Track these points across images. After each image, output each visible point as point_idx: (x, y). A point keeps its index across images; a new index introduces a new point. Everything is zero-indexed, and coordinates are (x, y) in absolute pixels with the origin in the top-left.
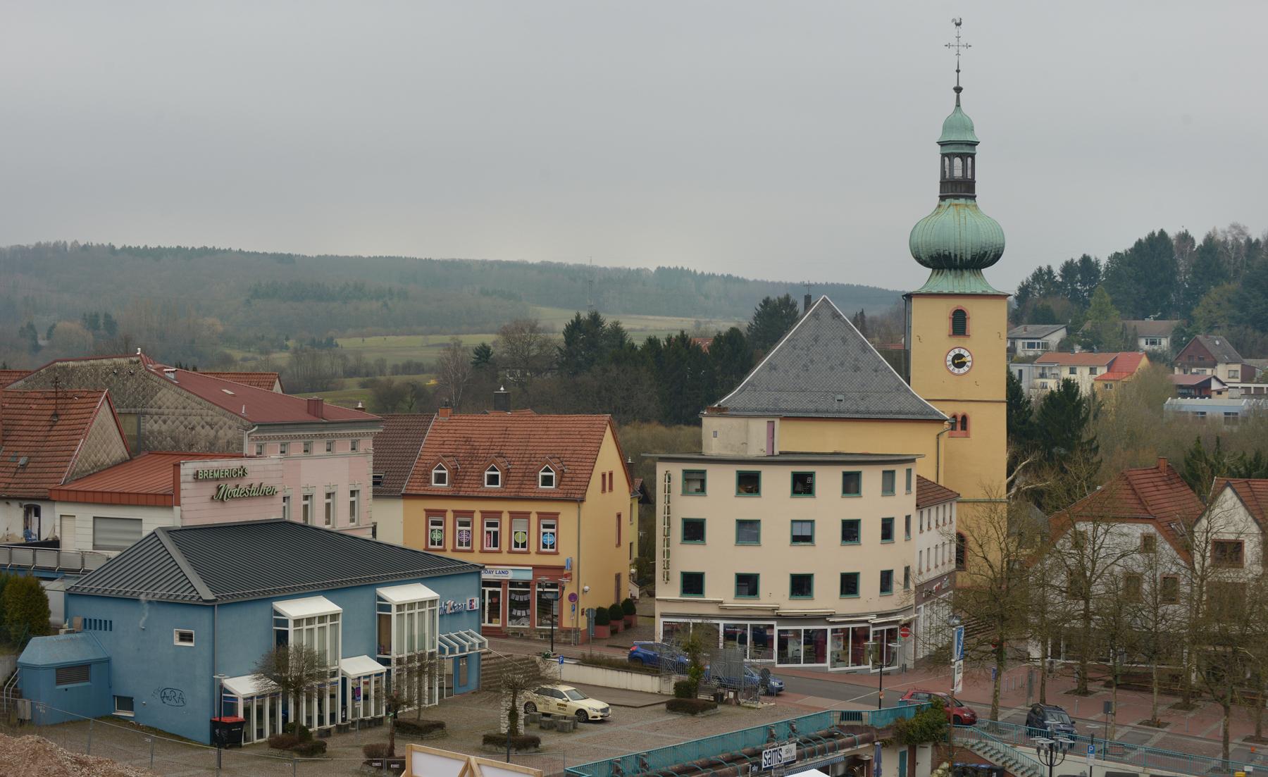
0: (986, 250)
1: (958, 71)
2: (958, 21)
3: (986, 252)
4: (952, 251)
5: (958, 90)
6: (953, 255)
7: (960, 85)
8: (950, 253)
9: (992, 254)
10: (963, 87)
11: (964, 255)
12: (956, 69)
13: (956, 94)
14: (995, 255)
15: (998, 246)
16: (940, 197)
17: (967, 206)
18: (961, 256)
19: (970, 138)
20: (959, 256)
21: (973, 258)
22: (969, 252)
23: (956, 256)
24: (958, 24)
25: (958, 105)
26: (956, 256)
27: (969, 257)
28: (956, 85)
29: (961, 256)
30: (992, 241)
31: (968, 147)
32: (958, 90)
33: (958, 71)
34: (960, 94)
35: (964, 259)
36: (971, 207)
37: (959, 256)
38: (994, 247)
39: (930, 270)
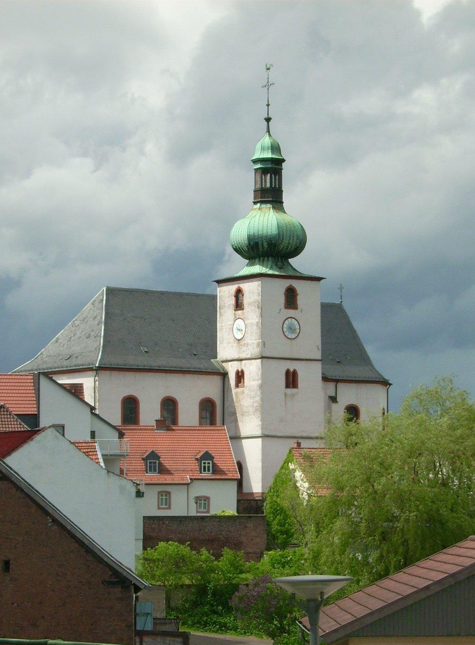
0: (257, 241)
2: (268, 66)
3: (257, 244)
5: (268, 120)
6: (238, 248)
9: (265, 244)
10: (272, 117)
14: (269, 244)
15: (269, 237)
16: (253, 202)
17: (260, 209)
21: (248, 248)
23: (239, 248)
24: (268, 69)
25: (268, 131)
27: (247, 249)
28: (266, 116)
32: (268, 120)
33: (268, 105)
34: (270, 123)
36: (264, 210)
39: (248, 261)
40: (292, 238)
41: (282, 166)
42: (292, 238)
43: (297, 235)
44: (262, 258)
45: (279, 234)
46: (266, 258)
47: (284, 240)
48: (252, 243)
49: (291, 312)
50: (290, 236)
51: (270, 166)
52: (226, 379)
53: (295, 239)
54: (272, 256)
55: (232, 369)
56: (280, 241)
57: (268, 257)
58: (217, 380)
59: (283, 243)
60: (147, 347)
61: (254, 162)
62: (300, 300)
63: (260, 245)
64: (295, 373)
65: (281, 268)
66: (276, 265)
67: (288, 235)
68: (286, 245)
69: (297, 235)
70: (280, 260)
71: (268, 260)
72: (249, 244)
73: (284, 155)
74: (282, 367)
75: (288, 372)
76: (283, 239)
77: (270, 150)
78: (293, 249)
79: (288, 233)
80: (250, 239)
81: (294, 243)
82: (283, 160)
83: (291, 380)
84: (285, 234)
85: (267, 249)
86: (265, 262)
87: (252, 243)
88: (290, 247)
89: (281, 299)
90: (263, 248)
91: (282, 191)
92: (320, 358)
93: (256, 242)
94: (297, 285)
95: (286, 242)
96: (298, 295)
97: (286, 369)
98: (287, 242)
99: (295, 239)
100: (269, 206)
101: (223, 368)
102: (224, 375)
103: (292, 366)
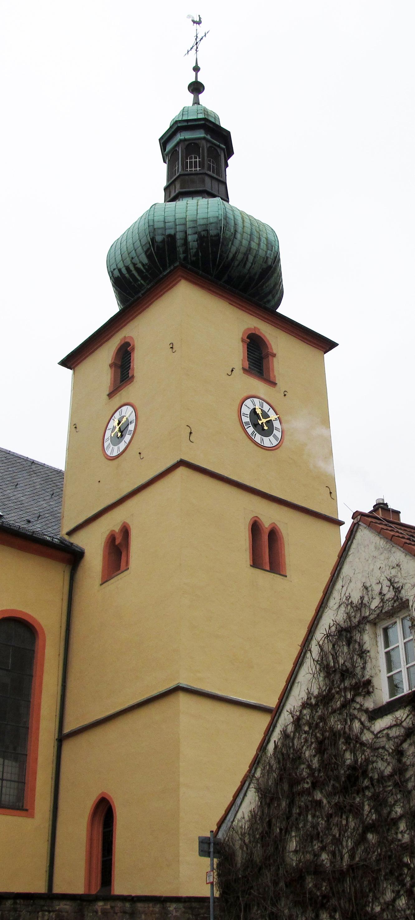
0: (172, 232)
3: (172, 238)
4: (121, 265)
6: (124, 271)
7: (199, 80)
8: (120, 270)
11: (136, 260)
18: (134, 265)
20: (132, 268)
21: (149, 256)
22: (140, 250)
26: (127, 268)
27: (145, 260)
29: (134, 265)
35: (140, 266)
37: (132, 268)
38: (189, 224)
40: (256, 240)
42: (256, 240)
47: (238, 236)
50: (251, 235)
52: (80, 573)
59: (237, 242)
63: (179, 242)
68: (243, 250)
72: (153, 239)
76: (236, 231)
80: (155, 229)
84: (240, 229)
85: (196, 254)
87: (159, 238)
88: (251, 258)
90: (186, 251)
93: (170, 236)
95: (241, 241)
96: (274, 355)
97: (251, 516)
98: (245, 242)
99: (263, 246)
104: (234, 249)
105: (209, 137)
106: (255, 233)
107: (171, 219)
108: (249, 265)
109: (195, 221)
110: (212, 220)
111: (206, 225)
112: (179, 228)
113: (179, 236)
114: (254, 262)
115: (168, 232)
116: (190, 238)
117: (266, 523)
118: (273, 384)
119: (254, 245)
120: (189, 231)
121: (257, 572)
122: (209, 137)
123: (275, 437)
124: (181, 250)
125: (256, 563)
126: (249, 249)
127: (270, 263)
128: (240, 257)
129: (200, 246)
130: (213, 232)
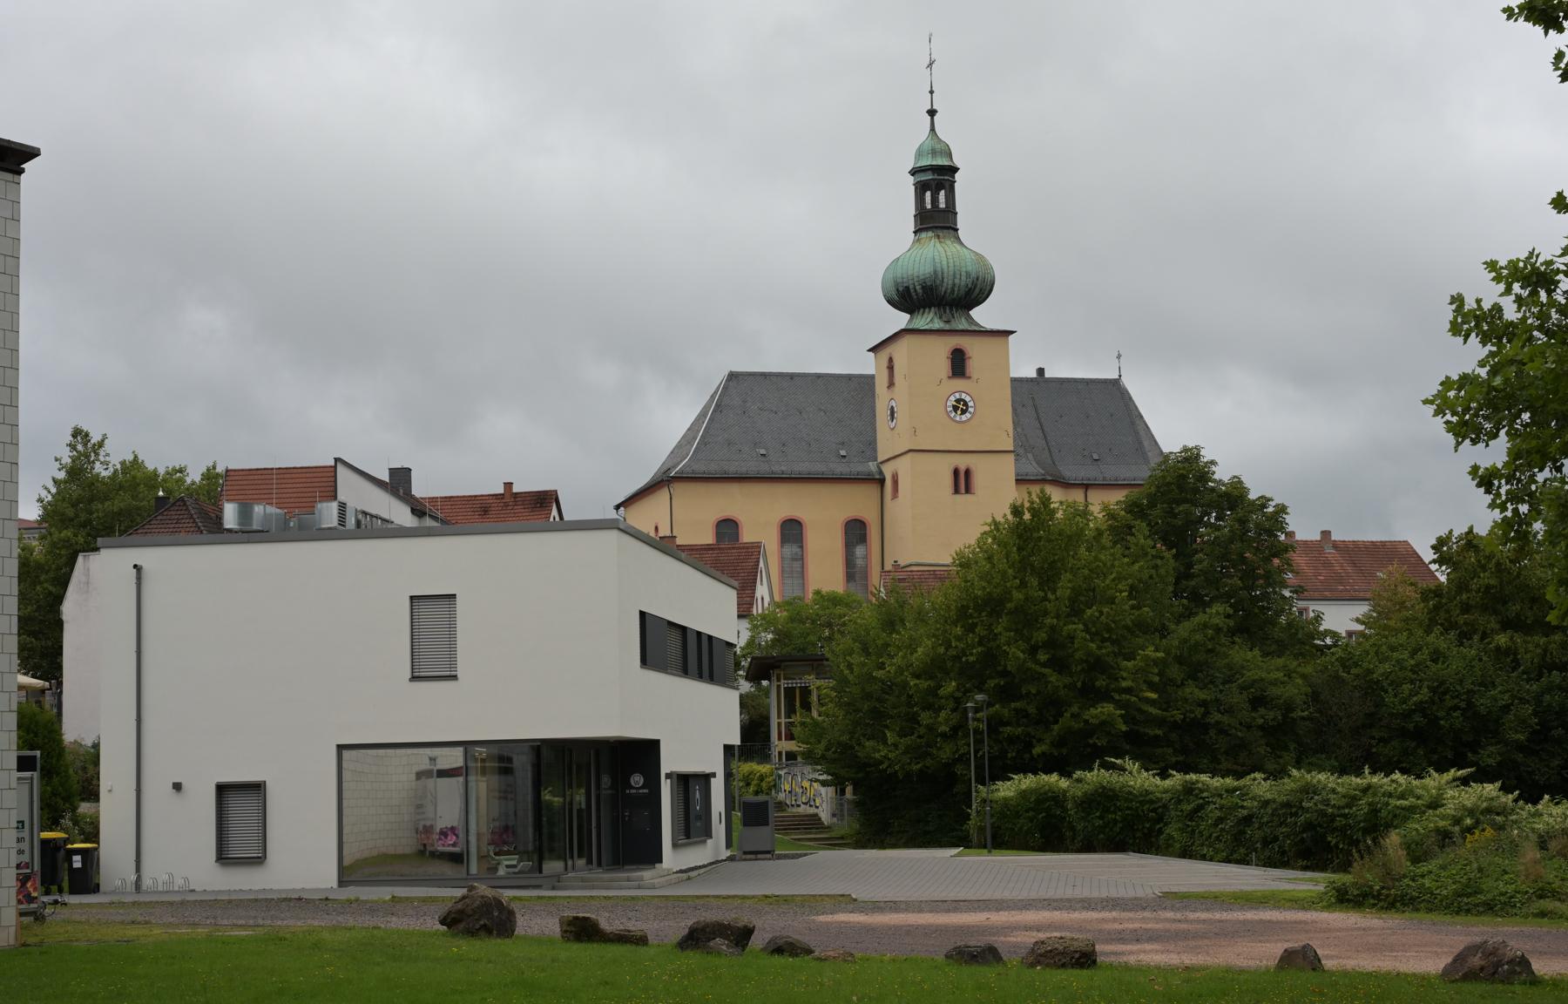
1: (932, 92)
3: (907, 288)
5: (932, 113)
7: (935, 107)
10: (938, 109)
12: (929, 89)
13: (929, 118)
14: (923, 288)
15: (922, 277)
19: (941, 161)
28: (930, 107)
30: (910, 273)
31: (922, 174)
32: (932, 113)
33: (932, 92)
34: (935, 117)
36: (922, 241)
40: (958, 277)
41: (954, 178)
43: (966, 272)
44: (922, 310)
45: (935, 272)
46: (927, 310)
47: (945, 280)
48: (901, 289)
49: (959, 384)
51: (930, 177)
53: (963, 278)
54: (935, 306)
55: (888, 471)
56: (938, 282)
57: (930, 308)
58: (873, 490)
59: (945, 284)
60: (766, 449)
61: (912, 175)
62: (974, 365)
63: (912, 291)
64: (967, 472)
65: (948, 322)
66: (941, 318)
67: (951, 273)
69: (966, 272)
70: (948, 311)
71: (929, 313)
72: (897, 290)
73: (957, 162)
74: (945, 466)
75: (956, 472)
76: (943, 278)
77: (930, 155)
78: (962, 292)
79: (951, 268)
81: (963, 283)
82: (955, 170)
83: (962, 482)
84: (946, 270)
86: (925, 315)
87: (901, 289)
88: (956, 289)
89: (944, 366)
90: (917, 295)
91: (957, 213)
92: (1012, 449)
94: (970, 345)
95: (948, 282)
98: (950, 282)
99: (963, 278)
100: (930, 234)
101: (881, 472)
102: (882, 481)
103: (962, 462)
104: (943, 289)
105: (936, 177)
106: (958, 272)
107: (905, 276)
108: (956, 292)
109: (918, 277)
110: (928, 276)
111: (924, 279)
112: (911, 282)
113: (911, 287)
114: (959, 290)
115: (905, 285)
116: (917, 288)
117: (962, 469)
118: (970, 377)
119: (957, 281)
120: (916, 284)
121: (958, 496)
122: (936, 177)
123: (970, 413)
124: (914, 294)
125: (957, 491)
126: (954, 285)
127: (970, 286)
128: (949, 291)
129: (924, 292)
130: (929, 284)
